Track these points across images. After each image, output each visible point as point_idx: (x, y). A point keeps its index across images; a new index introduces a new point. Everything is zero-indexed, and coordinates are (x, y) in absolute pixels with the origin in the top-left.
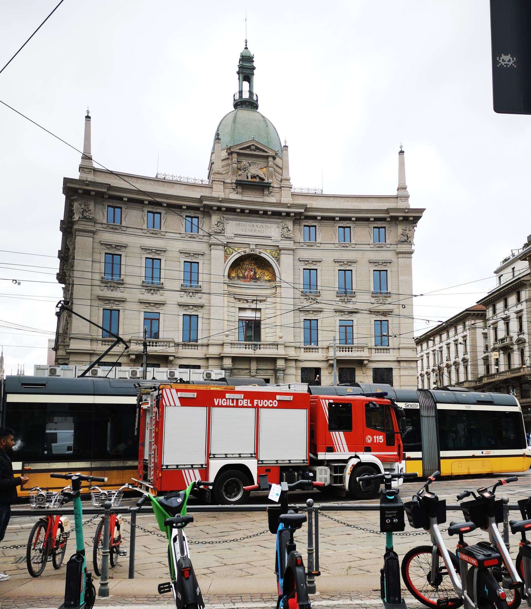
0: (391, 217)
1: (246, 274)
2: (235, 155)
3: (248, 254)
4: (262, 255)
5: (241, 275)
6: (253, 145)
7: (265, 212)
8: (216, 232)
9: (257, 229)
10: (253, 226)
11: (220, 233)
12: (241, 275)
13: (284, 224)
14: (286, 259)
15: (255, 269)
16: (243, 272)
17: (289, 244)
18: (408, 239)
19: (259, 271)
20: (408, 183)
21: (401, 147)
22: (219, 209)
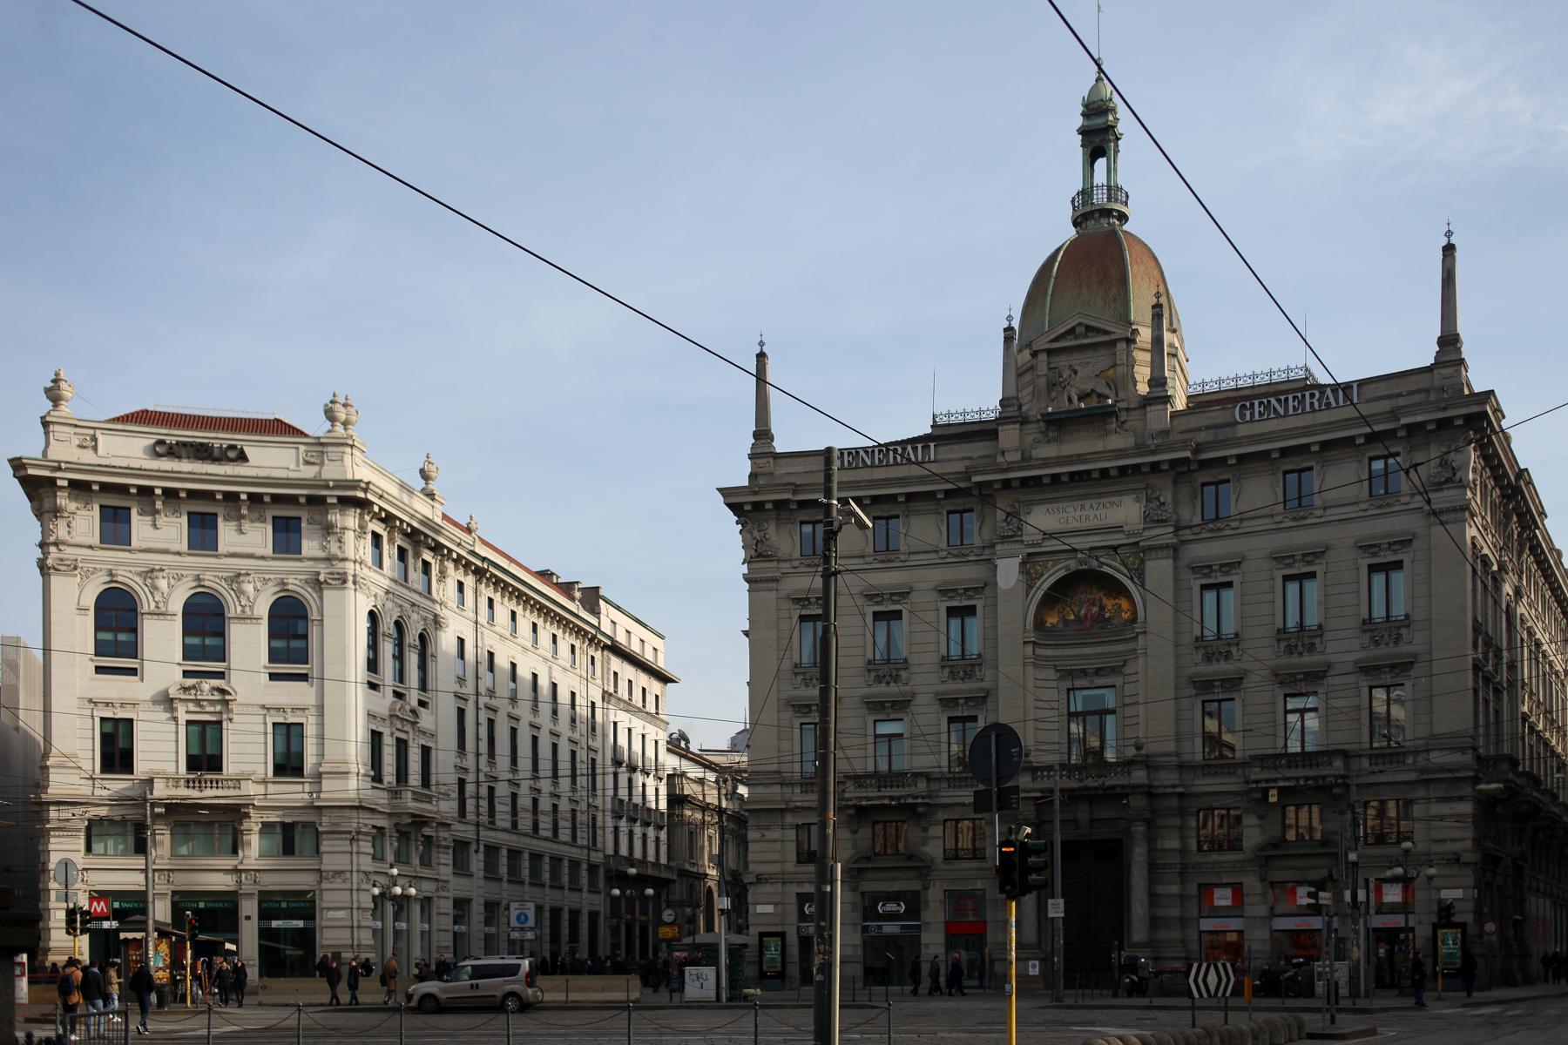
0: (1410, 428)
1: (1083, 612)
2: (1043, 357)
3: (1074, 572)
4: (1106, 569)
5: (1072, 617)
6: (1080, 324)
7: (1104, 473)
8: (1004, 537)
9: (1091, 513)
10: (1083, 507)
11: (1012, 536)
12: (1072, 617)
13: (1149, 492)
14: (1159, 570)
15: (1101, 600)
16: (1076, 610)
17: (1164, 534)
18: (1454, 474)
19: (1109, 603)
20: (1462, 328)
21: (1449, 234)
22: (1006, 484)
